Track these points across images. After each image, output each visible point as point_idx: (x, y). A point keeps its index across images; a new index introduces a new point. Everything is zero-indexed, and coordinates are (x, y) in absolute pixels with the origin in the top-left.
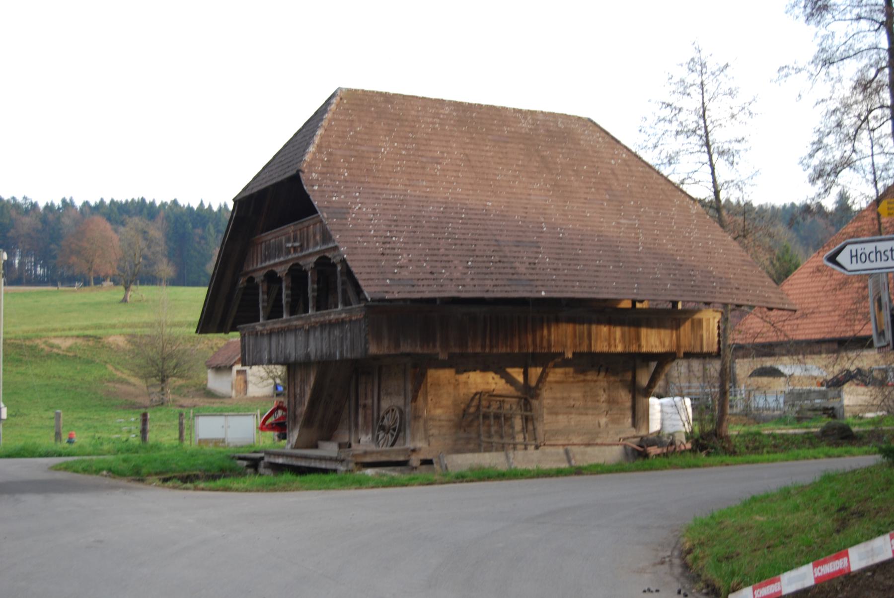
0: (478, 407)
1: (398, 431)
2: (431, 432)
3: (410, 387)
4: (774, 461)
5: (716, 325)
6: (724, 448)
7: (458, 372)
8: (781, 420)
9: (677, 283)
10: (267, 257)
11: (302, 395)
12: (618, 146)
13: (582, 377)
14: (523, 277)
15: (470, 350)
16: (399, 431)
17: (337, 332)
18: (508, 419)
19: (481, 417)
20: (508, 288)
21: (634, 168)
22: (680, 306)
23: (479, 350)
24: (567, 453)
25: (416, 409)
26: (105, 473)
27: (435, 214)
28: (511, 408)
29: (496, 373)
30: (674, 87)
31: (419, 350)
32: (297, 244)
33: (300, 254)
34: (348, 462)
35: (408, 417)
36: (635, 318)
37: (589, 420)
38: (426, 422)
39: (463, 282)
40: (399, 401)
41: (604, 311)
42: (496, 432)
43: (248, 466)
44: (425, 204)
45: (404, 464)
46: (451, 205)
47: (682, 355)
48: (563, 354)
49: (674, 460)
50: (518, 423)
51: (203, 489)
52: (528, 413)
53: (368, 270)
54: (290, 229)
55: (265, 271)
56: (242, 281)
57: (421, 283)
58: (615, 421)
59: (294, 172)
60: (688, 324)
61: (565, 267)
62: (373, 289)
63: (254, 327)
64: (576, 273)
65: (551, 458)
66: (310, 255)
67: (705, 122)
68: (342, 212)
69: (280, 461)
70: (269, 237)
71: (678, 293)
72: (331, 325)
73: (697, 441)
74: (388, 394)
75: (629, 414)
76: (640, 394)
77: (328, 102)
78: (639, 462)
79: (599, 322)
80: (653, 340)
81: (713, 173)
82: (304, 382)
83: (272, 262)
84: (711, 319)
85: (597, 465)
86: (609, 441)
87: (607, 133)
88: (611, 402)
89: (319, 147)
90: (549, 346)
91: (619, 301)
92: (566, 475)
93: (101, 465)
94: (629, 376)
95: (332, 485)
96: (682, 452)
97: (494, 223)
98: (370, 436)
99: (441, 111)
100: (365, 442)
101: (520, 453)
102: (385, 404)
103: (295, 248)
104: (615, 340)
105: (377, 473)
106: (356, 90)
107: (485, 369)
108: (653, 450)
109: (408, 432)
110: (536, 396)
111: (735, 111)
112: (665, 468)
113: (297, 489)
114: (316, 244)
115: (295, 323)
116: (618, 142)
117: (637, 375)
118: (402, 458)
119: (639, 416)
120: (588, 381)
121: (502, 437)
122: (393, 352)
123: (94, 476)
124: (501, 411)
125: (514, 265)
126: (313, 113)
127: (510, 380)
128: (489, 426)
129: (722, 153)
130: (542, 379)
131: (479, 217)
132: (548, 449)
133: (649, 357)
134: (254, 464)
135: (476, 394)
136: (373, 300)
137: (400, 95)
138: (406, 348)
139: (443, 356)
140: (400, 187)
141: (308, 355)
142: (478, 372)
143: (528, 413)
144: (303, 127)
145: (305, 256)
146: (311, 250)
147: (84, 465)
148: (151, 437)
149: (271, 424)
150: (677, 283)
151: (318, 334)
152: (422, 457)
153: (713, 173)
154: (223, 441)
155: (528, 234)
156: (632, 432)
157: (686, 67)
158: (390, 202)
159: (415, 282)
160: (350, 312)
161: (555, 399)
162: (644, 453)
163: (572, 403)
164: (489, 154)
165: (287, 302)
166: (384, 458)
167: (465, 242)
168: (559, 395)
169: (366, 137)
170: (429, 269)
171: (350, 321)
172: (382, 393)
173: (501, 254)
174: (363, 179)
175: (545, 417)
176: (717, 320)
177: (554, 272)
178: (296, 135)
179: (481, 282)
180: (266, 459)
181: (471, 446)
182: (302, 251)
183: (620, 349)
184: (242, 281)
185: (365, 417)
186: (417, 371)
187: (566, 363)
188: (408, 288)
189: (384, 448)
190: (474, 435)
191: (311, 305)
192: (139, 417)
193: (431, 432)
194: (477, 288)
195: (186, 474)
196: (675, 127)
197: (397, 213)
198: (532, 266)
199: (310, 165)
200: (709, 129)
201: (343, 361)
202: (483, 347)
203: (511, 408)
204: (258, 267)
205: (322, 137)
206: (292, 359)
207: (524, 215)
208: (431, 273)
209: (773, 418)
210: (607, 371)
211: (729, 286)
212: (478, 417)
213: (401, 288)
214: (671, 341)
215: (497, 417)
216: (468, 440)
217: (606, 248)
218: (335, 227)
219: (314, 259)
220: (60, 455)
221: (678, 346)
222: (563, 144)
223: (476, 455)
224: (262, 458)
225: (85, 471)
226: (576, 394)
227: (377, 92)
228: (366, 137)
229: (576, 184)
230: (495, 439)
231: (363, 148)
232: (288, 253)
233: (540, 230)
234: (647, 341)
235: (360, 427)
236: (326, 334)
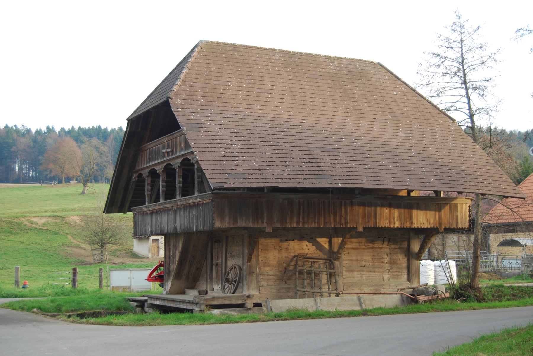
0: (296, 265)
2: (262, 283)
3: (246, 251)
4: (509, 306)
5: (468, 208)
6: (476, 296)
7: (282, 241)
8: (520, 276)
9: (438, 178)
10: (151, 160)
11: (174, 257)
12: (399, 82)
13: (371, 245)
14: (326, 173)
15: (288, 225)
16: (239, 282)
17: (194, 212)
18: (317, 274)
19: (297, 273)
20: (314, 181)
21: (410, 98)
22: (442, 195)
23: (295, 225)
24: (359, 299)
25: (250, 267)
26: (35, 310)
27: (265, 129)
28: (319, 267)
29: (309, 242)
30: (441, 43)
31: (251, 225)
32: (169, 150)
33: (171, 157)
34: (202, 304)
35: (245, 273)
36: (409, 203)
37: (376, 276)
38: (257, 276)
39: (282, 176)
40: (239, 261)
41: (388, 198)
42: (308, 284)
44: (258, 121)
45: (241, 306)
46: (276, 122)
47: (443, 230)
49: (435, 305)
50: (324, 278)
51: (92, 324)
52: (332, 271)
53: (213, 167)
54: (165, 139)
55: (149, 169)
56: (135, 176)
57: (251, 176)
58: (395, 277)
59: (165, 99)
60: (447, 208)
61: (357, 166)
62: (215, 181)
63: (142, 209)
64: (365, 170)
65: (347, 303)
66: (177, 157)
67: (463, 67)
68: (198, 127)
69: (157, 303)
70: (152, 146)
71: (439, 185)
72: (191, 207)
73: (457, 290)
74: (233, 256)
75: (405, 271)
76: (413, 257)
77: (192, 51)
78: (414, 306)
79: (382, 206)
80: (422, 219)
81: (469, 103)
82: (175, 247)
83: (154, 163)
84: (464, 206)
85: (381, 308)
87: (392, 73)
88: (392, 263)
89: (184, 81)
90: (346, 223)
92: (355, 316)
93: (34, 305)
95: (184, 322)
96: (443, 299)
97: (307, 135)
98: (220, 286)
99: (274, 57)
100: (216, 291)
101: (325, 299)
102: (230, 264)
103: (168, 152)
104: (394, 219)
105: (221, 312)
106: (212, 42)
107: (301, 239)
108: (422, 298)
109: (245, 283)
110: (338, 259)
111: (484, 59)
112: (429, 311)
113: (158, 324)
114: (181, 150)
115: (167, 205)
116: (399, 79)
117: (411, 243)
118: (240, 302)
119: (412, 273)
120: (376, 248)
121: (312, 288)
122: (232, 226)
123: (25, 313)
124: (312, 269)
125: (319, 165)
126: (182, 58)
127: (319, 247)
128: (303, 279)
129: (475, 89)
130: (342, 246)
131: (297, 131)
132: (346, 297)
133: (419, 231)
134: (141, 304)
135: (294, 256)
136: (215, 189)
137: (244, 46)
138: (242, 223)
139: (268, 230)
140: (240, 109)
141: (175, 228)
142: (296, 241)
143: (332, 271)
144: (176, 68)
145: (174, 158)
146: (178, 154)
147: (21, 304)
148: (79, 286)
149: (155, 276)
150: (438, 178)
151: (182, 213)
152: (255, 302)
153: (469, 103)
155: (331, 143)
156: (407, 284)
157: (450, 29)
158: (232, 120)
159: (247, 176)
160: (202, 197)
161: (351, 260)
162: (416, 300)
163: (364, 263)
164: (306, 87)
165: (163, 191)
166: (227, 302)
167: (285, 148)
168: (354, 258)
169: (218, 75)
170: (257, 167)
171: (203, 203)
172: (228, 256)
173: (310, 156)
174: (214, 104)
175: (345, 273)
176: (468, 205)
177: (348, 170)
178: (170, 74)
179: (295, 177)
180: (149, 302)
181: (290, 294)
182: (172, 155)
183: (397, 225)
184: (135, 176)
185: (217, 273)
186: (252, 239)
187: (359, 235)
188: (242, 180)
189: (228, 295)
190: (292, 286)
192: (71, 271)
193: (262, 283)
194: (292, 181)
195: (92, 311)
196: (442, 70)
197: (237, 127)
198: (333, 165)
199: (177, 94)
200: (466, 71)
201: (198, 232)
202: (298, 223)
203: (319, 267)
205: (186, 74)
206: (166, 231)
207: (329, 129)
208: (259, 170)
209: (514, 274)
210: (389, 241)
211: (476, 180)
212: (295, 274)
213: (235, 180)
214: (435, 220)
215: (309, 273)
216: (288, 290)
217: (388, 153)
218: (192, 137)
219: (180, 160)
220: (16, 297)
221: (440, 224)
223: (293, 300)
224: (146, 301)
225: (22, 309)
226: (367, 256)
227: (228, 44)
228: (218, 75)
229: (368, 108)
230: (308, 289)
231: (215, 82)
232: (164, 156)
233: (340, 140)
234: (417, 220)
235: (214, 280)
236: (187, 214)
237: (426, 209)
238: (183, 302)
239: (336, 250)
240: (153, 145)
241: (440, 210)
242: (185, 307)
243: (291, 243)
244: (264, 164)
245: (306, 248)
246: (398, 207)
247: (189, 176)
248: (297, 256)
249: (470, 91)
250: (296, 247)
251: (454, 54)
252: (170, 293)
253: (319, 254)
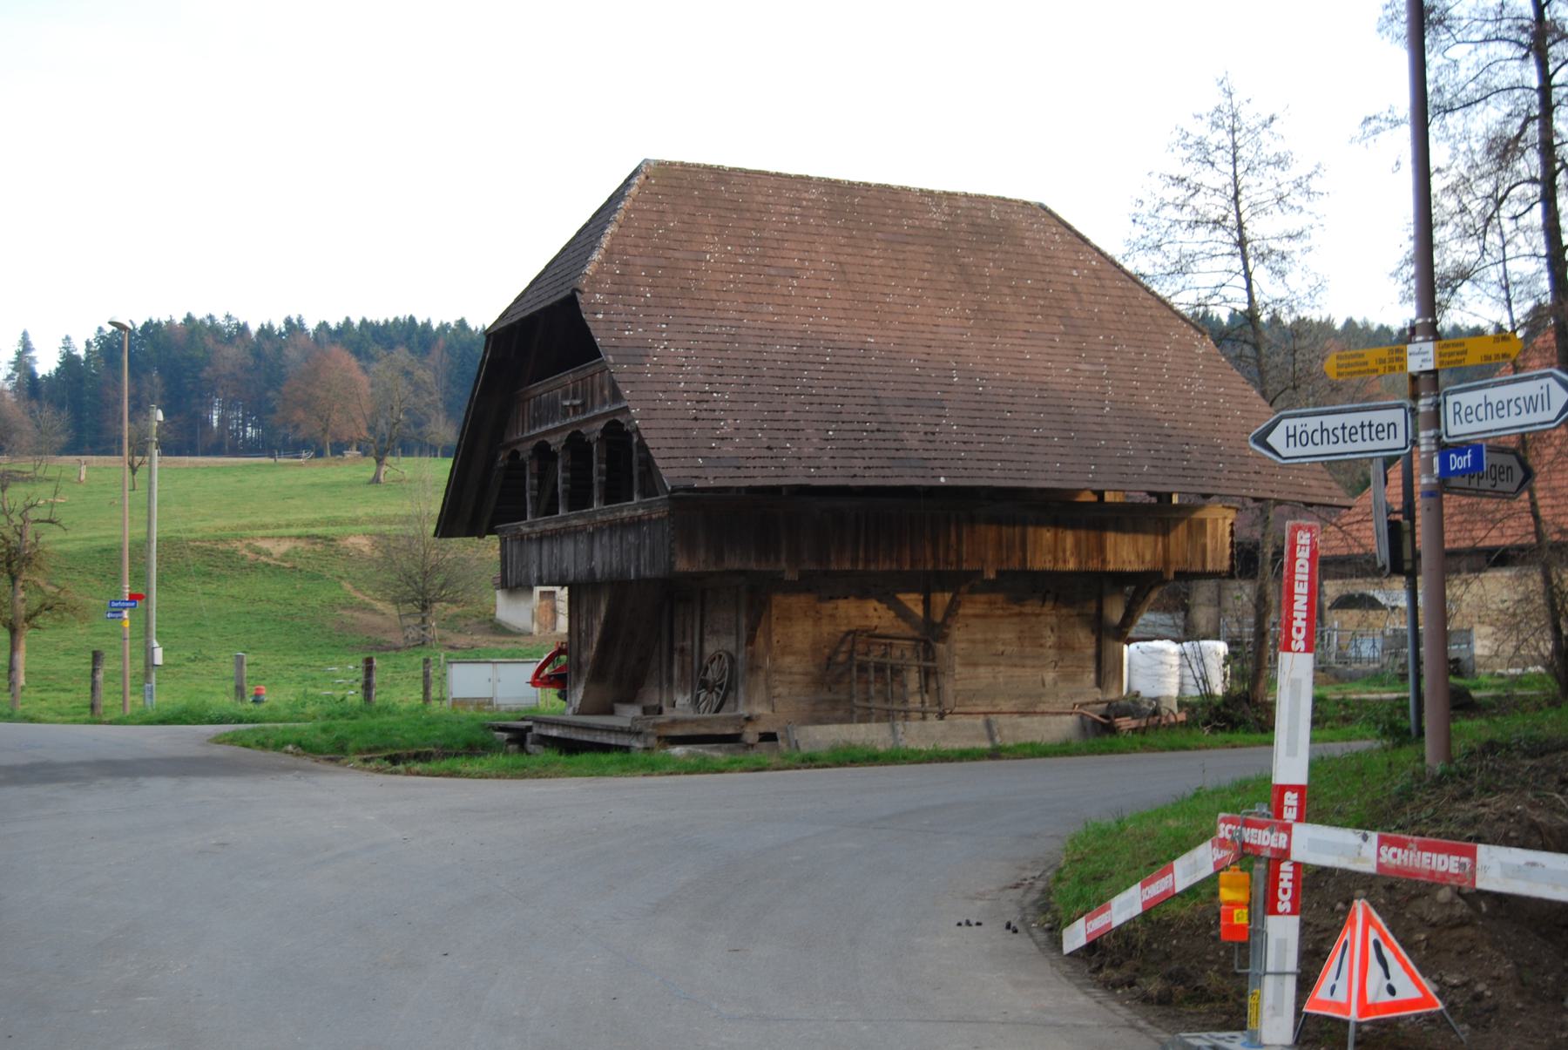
0: (851, 653)
1: (726, 690)
2: (777, 691)
3: (743, 622)
5: (1228, 529)
6: (1259, 720)
7: (821, 600)
8: (1376, 678)
9: (1159, 463)
11: (589, 634)
12: (1085, 248)
13: (1016, 609)
14: (913, 454)
15: (834, 567)
16: (729, 688)
17: (631, 538)
18: (897, 672)
19: (855, 669)
20: (887, 472)
21: (1108, 283)
22: (1175, 500)
23: (847, 566)
24: (988, 725)
25: (753, 655)
26: (290, 748)
27: (783, 357)
28: (903, 656)
29: (880, 601)
30: (1187, 154)
31: (753, 566)
32: (577, 402)
33: (581, 418)
34: (649, 735)
35: (741, 669)
36: (1098, 517)
39: (818, 463)
40: (728, 644)
41: (1057, 508)
42: (879, 692)
43: (510, 741)
44: (769, 340)
45: (734, 739)
46: (809, 343)
47: (1171, 576)
48: (981, 572)
49: (1150, 739)
50: (913, 679)
51: (418, 774)
52: (930, 664)
53: (671, 443)
54: (568, 378)
55: (534, 443)
57: (751, 463)
58: (1068, 677)
59: (568, 292)
60: (1182, 529)
61: (982, 438)
62: (674, 473)
63: (519, 529)
64: (999, 448)
65: (964, 732)
66: (595, 418)
67: (1237, 208)
68: (639, 353)
69: (554, 732)
70: (540, 390)
71: (1160, 479)
73: (1217, 708)
74: (714, 632)
75: (1092, 666)
77: (627, 183)
79: (1039, 523)
80: (1127, 552)
81: (1249, 288)
82: (592, 613)
83: (544, 428)
84: (1220, 525)
85: (1032, 745)
86: (1058, 707)
87: (1068, 227)
88: (1063, 647)
90: (959, 560)
91: (1079, 491)
92: (974, 759)
93: (288, 736)
94: (1091, 608)
95: (610, 770)
96: (1171, 726)
97: (874, 370)
99: (806, 195)
100: (682, 706)
101: (914, 726)
102: (710, 649)
103: (575, 407)
104: (1064, 551)
105: (690, 754)
106: (671, 164)
107: (864, 594)
108: (1125, 723)
109: (741, 690)
110: (943, 638)
111: (1284, 189)
112: (1134, 750)
113: (557, 775)
114: (604, 402)
115: (574, 522)
116: (1085, 241)
117: (1102, 607)
118: (730, 731)
119: (1106, 669)
120: (1026, 615)
121: (887, 700)
122: (713, 569)
123: (271, 753)
124: (888, 660)
125: (900, 436)
126: (605, 199)
127: (903, 613)
128: (867, 682)
129: (1262, 257)
130: (951, 610)
131: (853, 361)
133: (1120, 579)
134: (519, 737)
135: (848, 633)
136: (674, 489)
137: (741, 170)
138: (733, 563)
139: (791, 575)
140: (732, 314)
141: (592, 571)
142: (852, 599)
143: (930, 664)
144: (591, 221)
145: (588, 421)
146: (597, 411)
147: (260, 736)
148: (379, 699)
149: (549, 676)
150: (1159, 463)
151: (605, 539)
152: (763, 730)
153: (1249, 288)
154: (490, 701)
155: (928, 387)
156: (1098, 694)
157: (1208, 120)
158: (713, 338)
159: (742, 462)
160: (648, 506)
161: (973, 642)
162: (1117, 725)
163: (1001, 648)
164: (876, 262)
165: (564, 491)
166: (703, 731)
167: (827, 400)
168: (979, 636)
169: (683, 237)
170: (765, 442)
171: (650, 519)
172: (706, 631)
173: (881, 418)
174: (674, 302)
175: (958, 669)
176: (1229, 521)
177: (963, 447)
178: (579, 233)
179: (846, 463)
180: (536, 730)
181: (840, 713)
182: (584, 412)
183: (1071, 565)
185: (683, 668)
186: (756, 599)
187: (991, 587)
188: (732, 472)
189: (706, 715)
190: (844, 697)
191: (596, 494)
192: (360, 663)
193: (777, 691)
194: (840, 472)
195: (413, 751)
196: (1187, 215)
197: (723, 354)
198: (930, 437)
199: (593, 281)
200: (1244, 218)
201: (640, 580)
202: (855, 561)
203: (903, 656)
204: (526, 434)
205: (614, 236)
206: (571, 578)
207: (924, 357)
208: (769, 448)
209: (1365, 673)
210: (1056, 600)
211: (1244, 468)
212: (850, 670)
213: (718, 472)
214: (1154, 553)
215: (880, 669)
216: (834, 704)
217: (1051, 410)
218: (625, 377)
219: (601, 425)
220: (240, 721)
221: (1166, 562)
222: (999, 244)
223: (845, 726)
224: (529, 729)
225: (263, 745)
226: (1007, 633)
227: (705, 167)
228: (683, 237)
229: (1013, 308)
230: (877, 703)
231: (677, 255)
232: (566, 415)
233: (947, 381)
234: (1116, 554)
235: (676, 683)
236: (616, 540)
238: (610, 730)
239: (938, 619)
240: (542, 390)
242: (612, 740)
243: (842, 603)
244: (781, 435)
245: (876, 615)
246: (1073, 525)
247: (618, 459)
249: (1251, 262)
250: (853, 612)
251: (1218, 177)
253: (903, 628)
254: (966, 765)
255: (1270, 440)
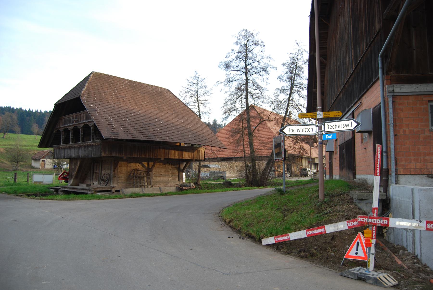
0: (134, 174)
1: (108, 181)
3: (113, 167)
4: (219, 192)
7: (128, 163)
10: (65, 124)
11: (75, 169)
13: (164, 166)
15: (133, 156)
17: (90, 149)
18: (143, 178)
23: (136, 156)
24: (160, 188)
31: (117, 155)
34: (92, 190)
37: (166, 179)
38: (117, 178)
40: (109, 172)
41: (172, 146)
43: (54, 191)
45: (110, 191)
48: (161, 158)
50: (145, 179)
51: (44, 199)
54: (74, 115)
56: (55, 131)
58: (173, 179)
65: (155, 190)
66: (81, 123)
68: (95, 110)
69: (67, 189)
72: (88, 146)
74: (104, 169)
75: (177, 177)
76: (181, 171)
78: (180, 192)
79: (172, 149)
80: (187, 155)
86: (172, 185)
87: (173, 94)
88: (173, 173)
89: (87, 89)
90: (157, 156)
91: (176, 143)
93: (3, 190)
94: (178, 166)
98: (97, 182)
100: (96, 184)
101: (146, 188)
102: (103, 172)
103: (75, 121)
107: (136, 162)
108: (185, 188)
109: (111, 181)
110: (151, 171)
113: (78, 200)
114: (84, 120)
116: (176, 97)
118: (109, 190)
121: (141, 183)
127: (144, 166)
128: (137, 180)
130: (153, 166)
132: (154, 187)
134: (57, 190)
136: (106, 139)
139: (125, 158)
140: (112, 104)
141: (79, 156)
151: (83, 149)
153: (199, 109)
154: (42, 182)
156: (178, 183)
166: (104, 190)
171: (95, 145)
178: (77, 85)
180: (61, 189)
181: (131, 186)
183: (177, 158)
184: (55, 131)
185: (96, 176)
186: (115, 163)
191: (80, 140)
195: (33, 193)
196: (189, 95)
199: (83, 94)
202: (137, 155)
204: (61, 126)
205: (87, 86)
206: (73, 157)
210: (172, 164)
213: (114, 135)
215: (139, 177)
218: (93, 115)
219: (83, 125)
221: (193, 158)
222: (160, 96)
224: (60, 189)
226: (163, 171)
230: (139, 184)
236: (86, 149)
237: (188, 151)
238: (80, 189)
239: (150, 167)
240: (67, 117)
241: (193, 152)
242: (81, 191)
243: (132, 164)
244: (126, 129)
245: (138, 166)
246: (178, 150)
247: (90, 131)
248: (134, 170)
249: (200, 104)
250: (134, 166)
251: (194, 89)
252: (72, 185)
253: (143, 169)
254: (162, 197)
255: (356, 124)
